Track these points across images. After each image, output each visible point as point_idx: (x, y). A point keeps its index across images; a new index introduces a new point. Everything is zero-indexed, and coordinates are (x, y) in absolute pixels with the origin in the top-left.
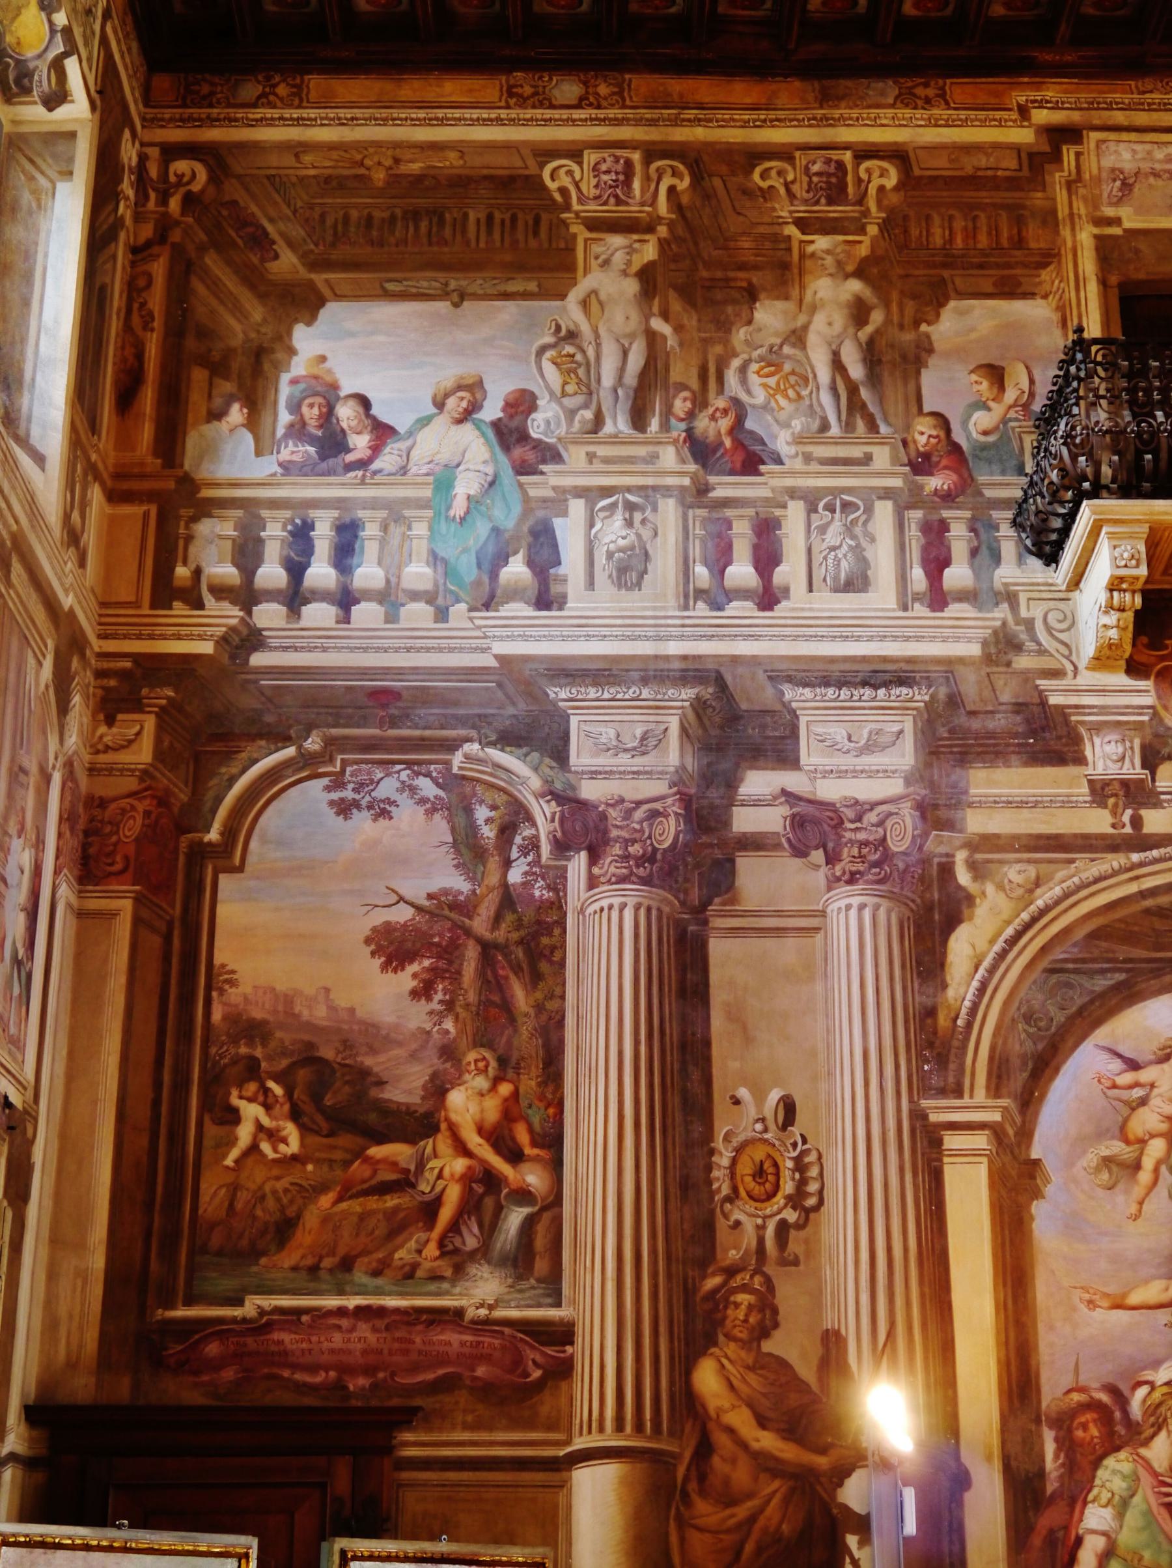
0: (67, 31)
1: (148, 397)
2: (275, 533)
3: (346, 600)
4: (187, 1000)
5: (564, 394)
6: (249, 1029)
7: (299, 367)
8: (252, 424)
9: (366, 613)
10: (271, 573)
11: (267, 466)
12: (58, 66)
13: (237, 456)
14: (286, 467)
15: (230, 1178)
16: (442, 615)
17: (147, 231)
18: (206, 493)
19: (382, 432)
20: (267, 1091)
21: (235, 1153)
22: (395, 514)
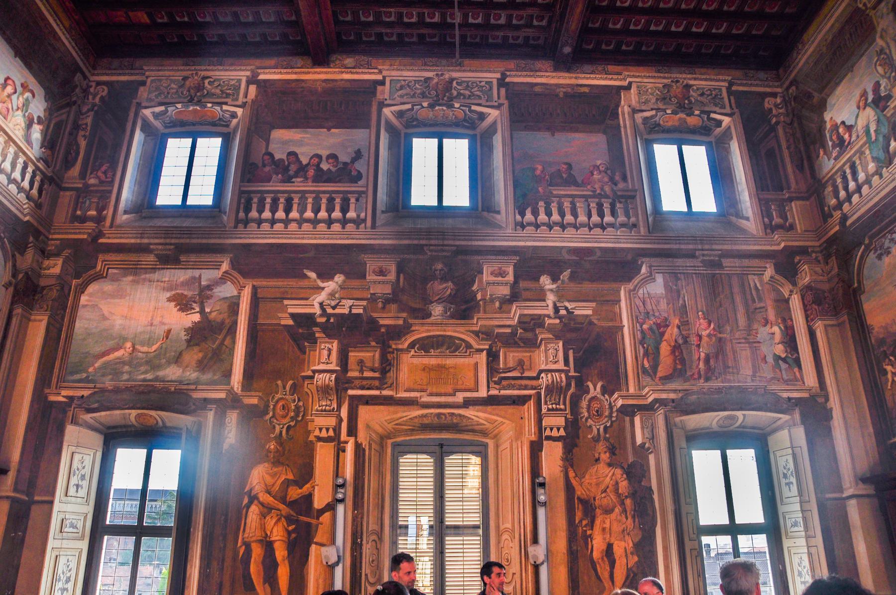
0: (702, 112)
1: (806, 163)
2: (839, 180)
3: (859, 189)
4: (865, 339)
5: (885, 73)
6: (882, 342)
7: (828, 126)
8: (825, 153)
9: (865, 189)
10: (842, 194)
11: (832, 161)
12: (709, 119)
13: (828, 165)
14: (835, 159)
15: (890, 392)
16: (881, 176)
17: (791, 116)
18: (824, 181)
19: (849, 128)
20: (890, 360)
21: (889, 384)
22: (860, 152)
